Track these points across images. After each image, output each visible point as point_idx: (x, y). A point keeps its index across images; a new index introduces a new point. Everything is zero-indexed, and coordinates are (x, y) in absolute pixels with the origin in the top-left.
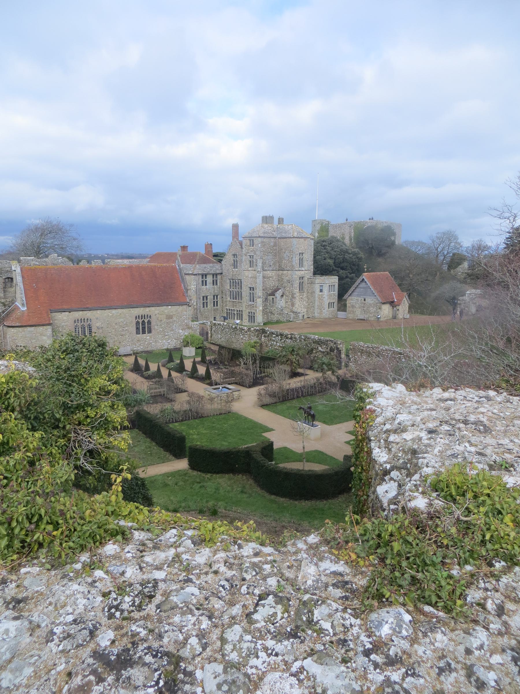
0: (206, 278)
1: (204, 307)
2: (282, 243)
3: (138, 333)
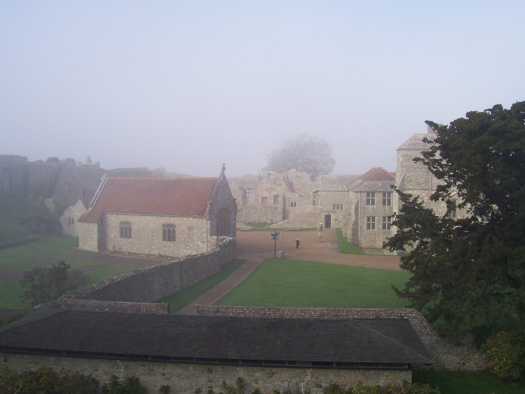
0: (373, 196)
1: (368, 228)
3: (164, 240)
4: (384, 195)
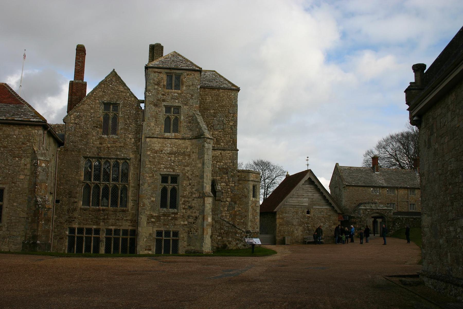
2: (209, 99)
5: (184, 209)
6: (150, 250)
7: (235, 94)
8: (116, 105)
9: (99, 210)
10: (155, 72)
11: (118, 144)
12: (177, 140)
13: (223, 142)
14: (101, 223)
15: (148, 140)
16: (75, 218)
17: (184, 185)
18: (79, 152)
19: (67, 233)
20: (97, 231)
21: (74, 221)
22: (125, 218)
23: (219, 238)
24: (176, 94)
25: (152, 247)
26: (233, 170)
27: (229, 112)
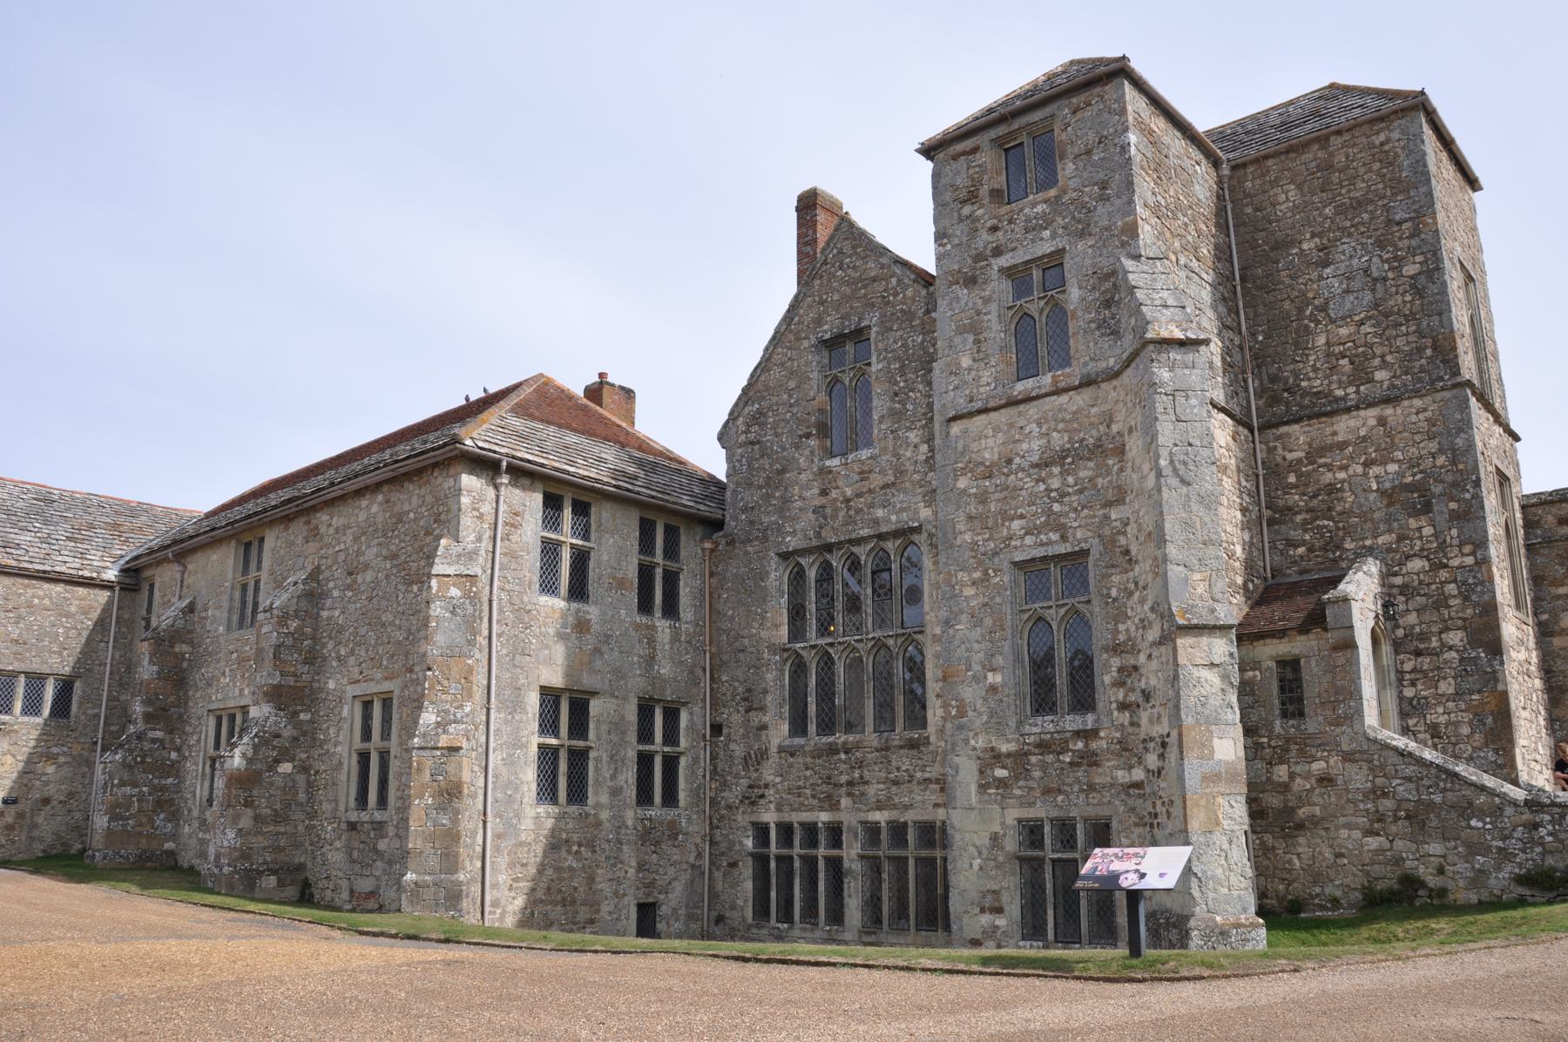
2: (1287, 198)
4: (646, 545)
5: (1123, 706)
6: (998, 910)
7: (1404, 132)
8: (859, 335)
9: (832, 750)
10: (955, 158)
11: (876, 480)
12: (1064, 398)
13: (1385, 365)
14: (845, 802)
15: (956, 429)
16: (766, 786)
17: (1114, 592)
18: (765, 539)
19: (749, 843)
20: (835, 832)
21: (762, 796)
22: (919, 775)
23: (1373, 843)
24: (1039, 209)
25: (1005, 898)
26: (1455, 484)
27: (1389, 221)
